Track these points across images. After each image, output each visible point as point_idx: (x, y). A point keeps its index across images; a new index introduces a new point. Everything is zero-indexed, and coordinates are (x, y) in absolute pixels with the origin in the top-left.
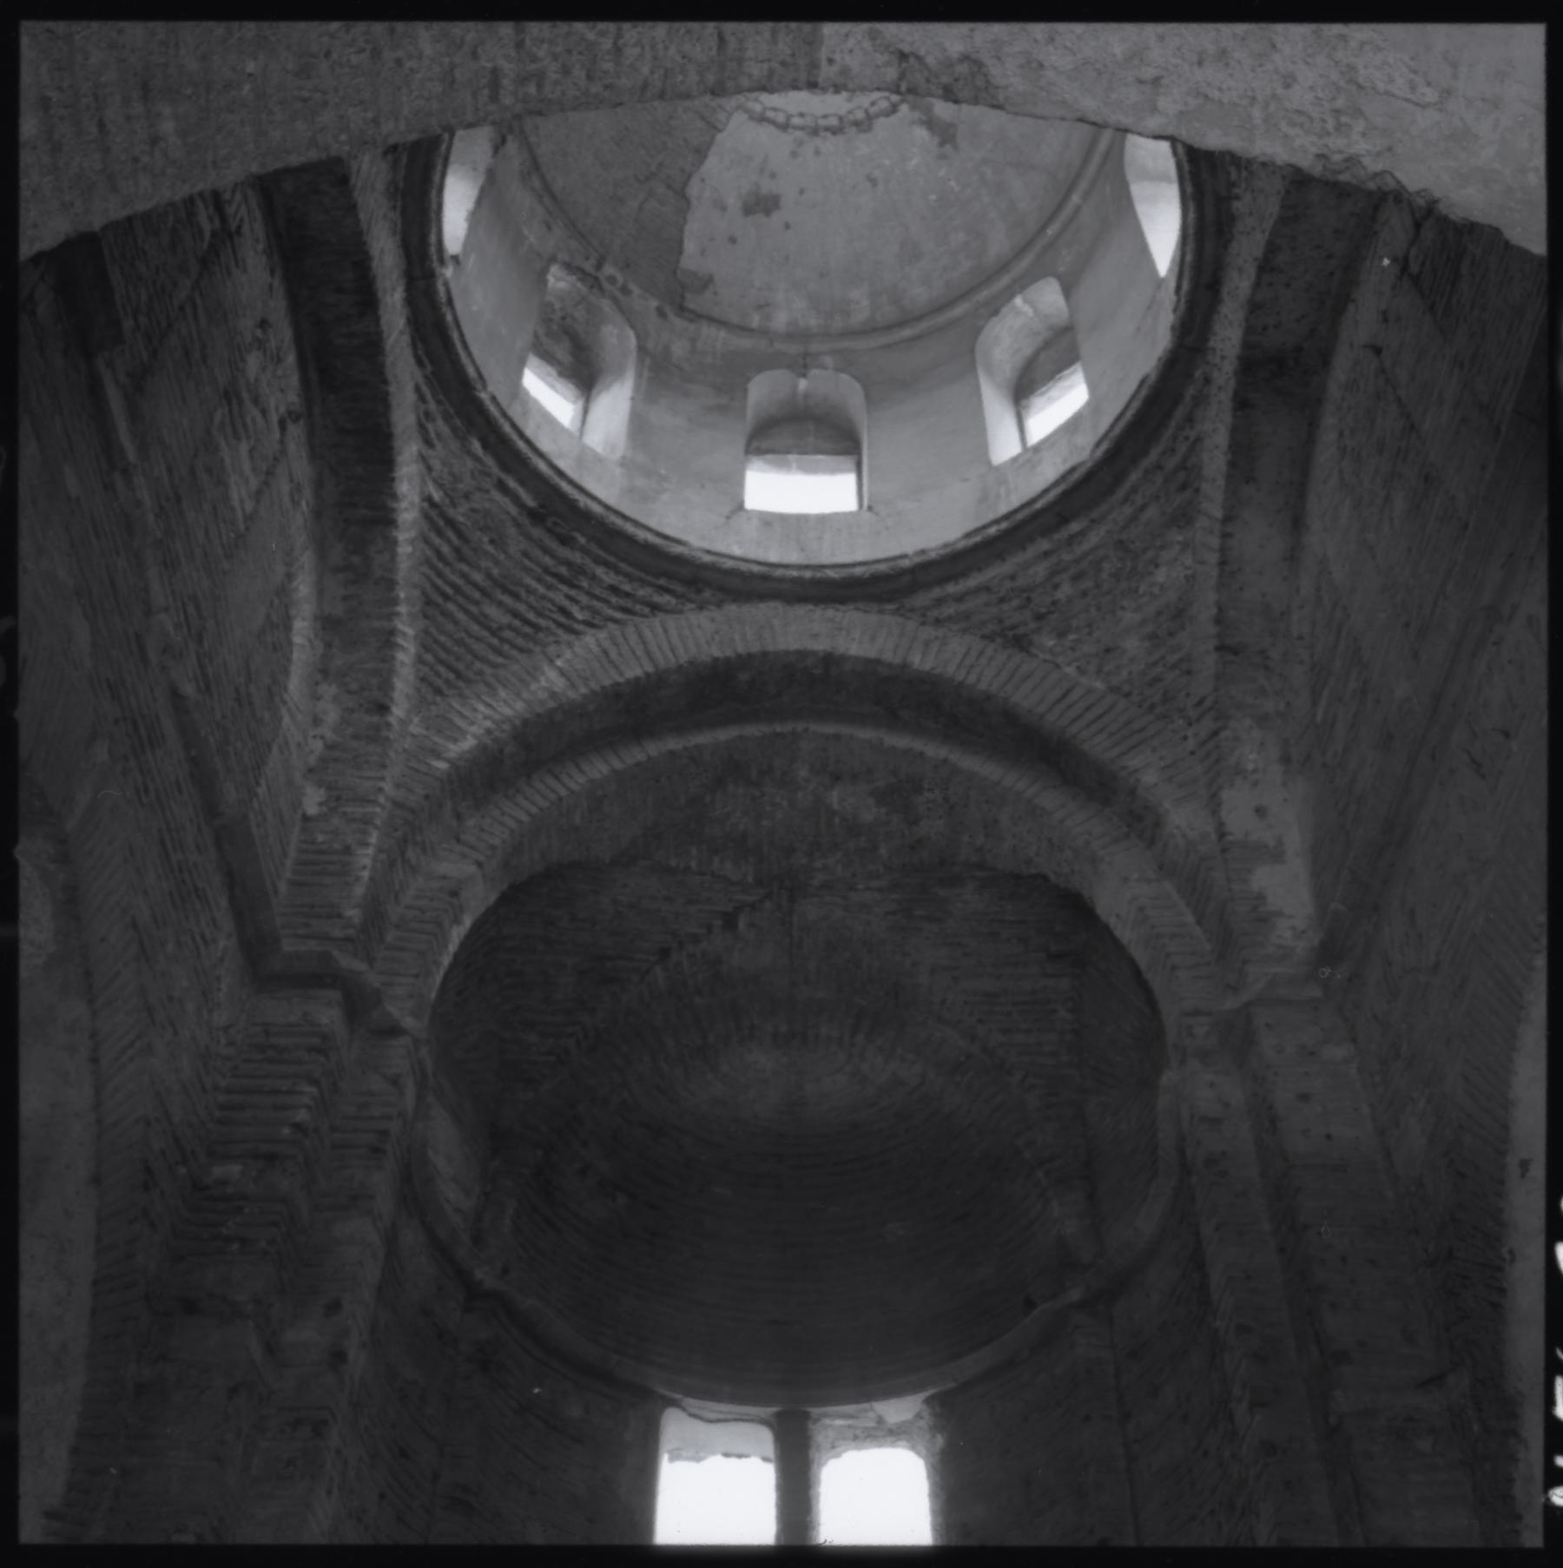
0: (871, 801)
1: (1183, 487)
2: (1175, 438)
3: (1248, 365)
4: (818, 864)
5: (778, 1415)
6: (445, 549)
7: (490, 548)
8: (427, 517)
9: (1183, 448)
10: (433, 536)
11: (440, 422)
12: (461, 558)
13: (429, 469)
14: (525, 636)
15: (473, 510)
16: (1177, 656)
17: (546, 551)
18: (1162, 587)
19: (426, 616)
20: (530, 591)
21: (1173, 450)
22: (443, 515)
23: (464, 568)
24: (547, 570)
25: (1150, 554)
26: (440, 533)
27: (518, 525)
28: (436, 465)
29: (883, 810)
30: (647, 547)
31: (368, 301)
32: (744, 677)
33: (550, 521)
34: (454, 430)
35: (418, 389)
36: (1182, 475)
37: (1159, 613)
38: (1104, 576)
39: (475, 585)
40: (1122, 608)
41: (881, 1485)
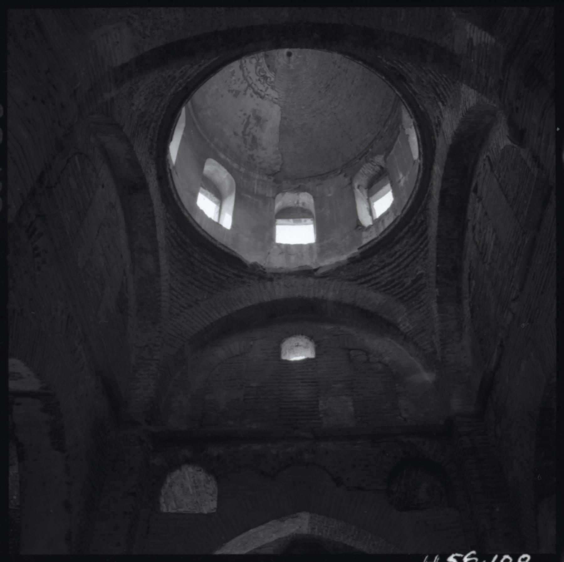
6: (442, 89)
7: (423, 80)
8: (446, 101)
11: (433, 121)
13: (440, 112)
23: (436, 81)
26: (443, 94)
31: (443, 194)
35: (438, 135)
39: (432, 74)
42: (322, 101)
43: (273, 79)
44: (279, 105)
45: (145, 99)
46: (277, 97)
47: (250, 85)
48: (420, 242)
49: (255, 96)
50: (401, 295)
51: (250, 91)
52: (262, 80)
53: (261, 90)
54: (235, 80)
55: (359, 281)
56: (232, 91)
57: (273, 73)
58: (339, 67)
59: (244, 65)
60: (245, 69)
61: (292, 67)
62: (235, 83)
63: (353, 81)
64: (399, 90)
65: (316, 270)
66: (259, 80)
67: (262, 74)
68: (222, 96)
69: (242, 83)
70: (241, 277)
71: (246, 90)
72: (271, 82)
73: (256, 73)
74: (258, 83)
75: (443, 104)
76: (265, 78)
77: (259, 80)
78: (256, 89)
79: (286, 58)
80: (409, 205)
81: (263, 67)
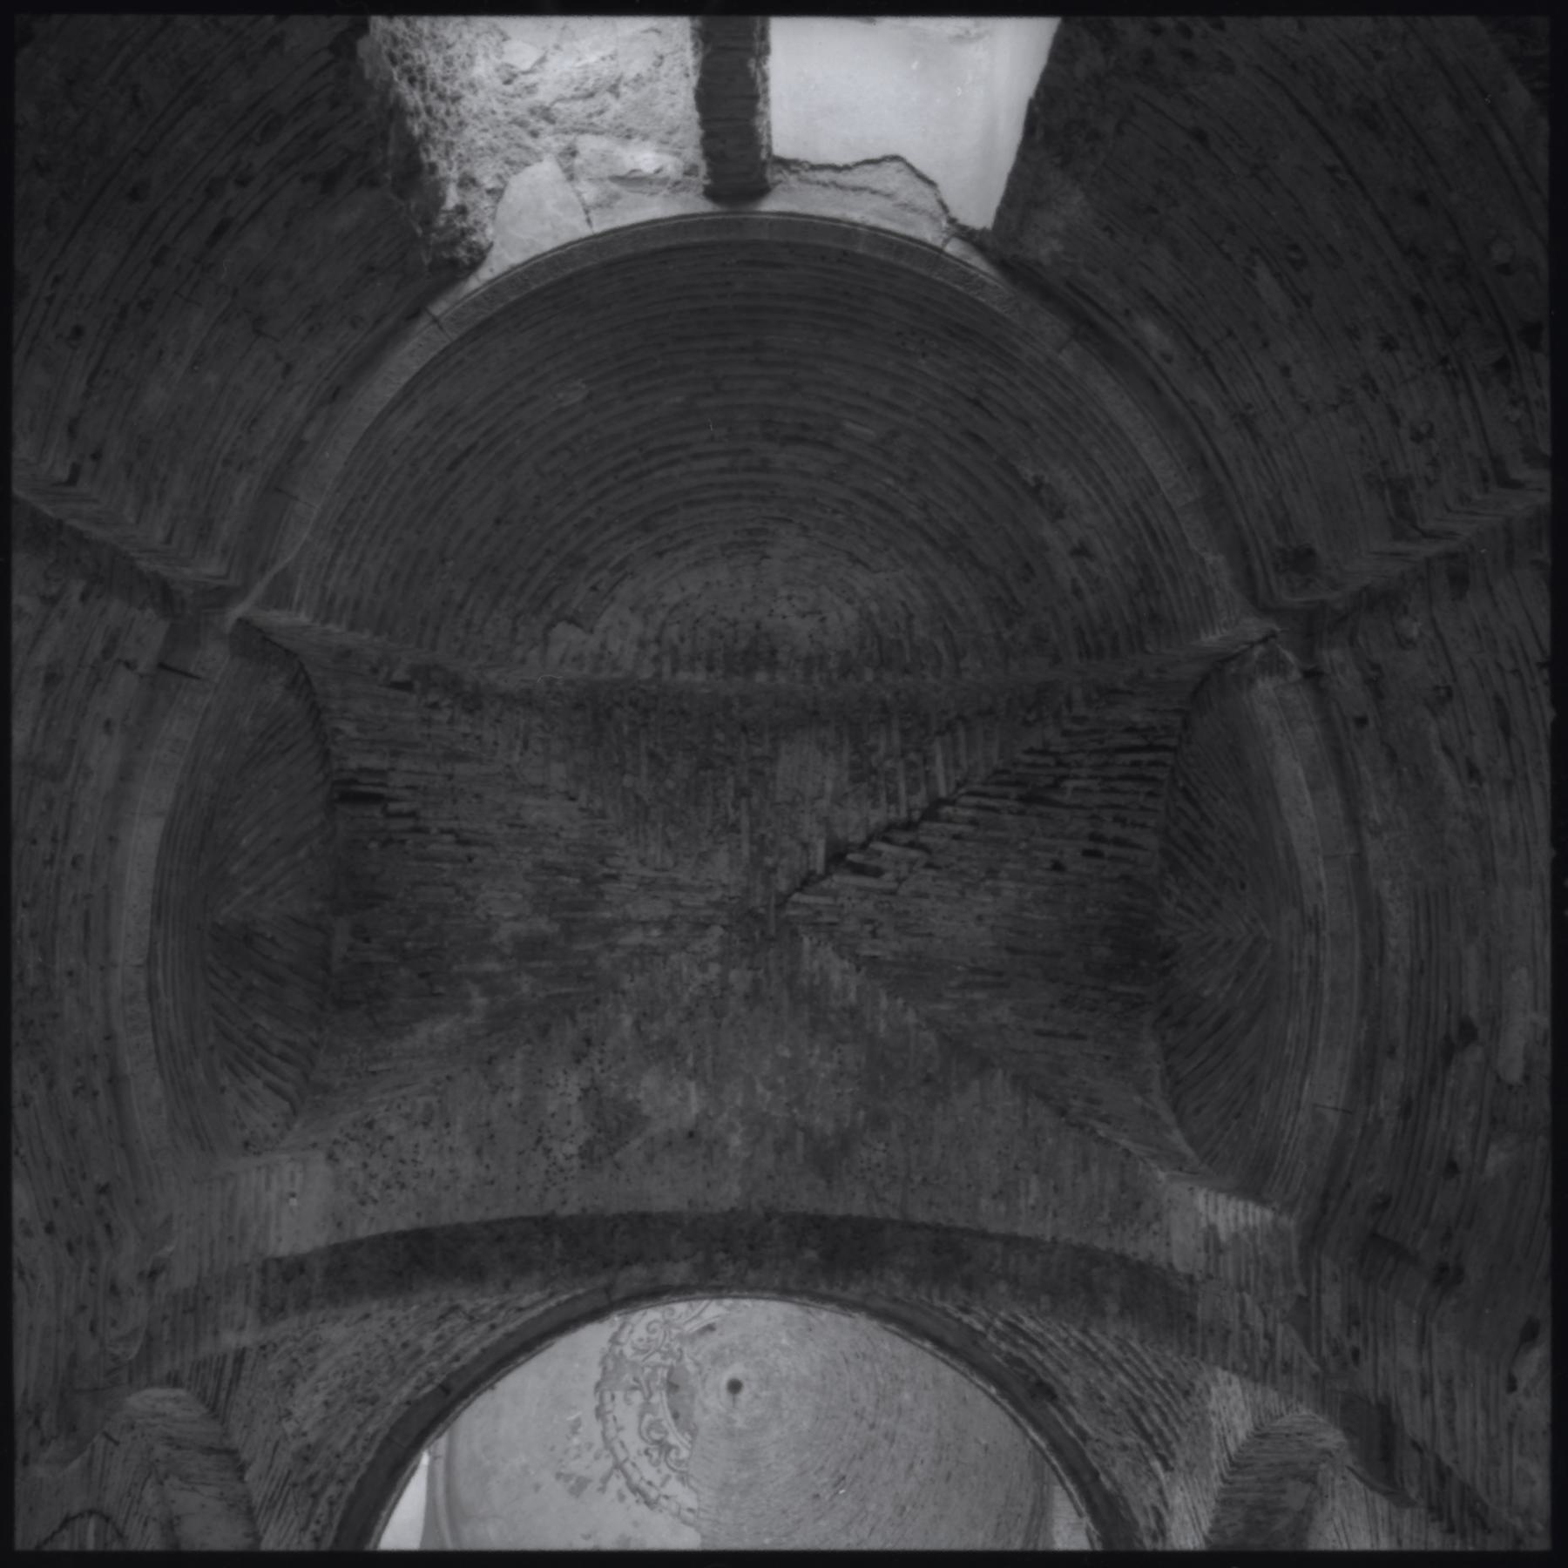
0: (647, 1109)
1: (311, 1479)
2: (331, 1514)
4: (715, 969)
5: (763, 190)
6: (1156, 1417)
7: (1104, 1393)
8: (1173, 1455)
9: (322, 1508)
10: (1169, 1436)
11: (1142, 1522)
12: (1138, 1400)
13: (1160, 1492)
15: (1118, 1433)
16: (282, 1349)
17: (1040, 1363)
18: (316, 1391)
19: (1192, 1385)
20: (1066, 1341)
21: (331, 1503)
22: (1154, 1447)
23: (1138, 1393)
24: (1042, 1349)
25: (337, 1408)
26: (1161, 1434)
27: (1072, 1400)
28: (1151, 1490)
29: (630, 1096)
30: (925, 1335)
32: (811, 1255)
33: (1033, 1379)
34: (1128, 1508)
36: (315, 1487)
37: (312, 1369)
38: (385, 1370)
39: (1127, 1374)
40: (358, 1354)
41: (558, 133)
42: (822, 1523)
43: (684, 1454)
44: (698, 1529)
45: (326, 1404)
46: (693, 1504)
47: (618, 1466)
49: (631, 1498)
51: (617, 1483)
52: (655, 1454)
53: (650, 1483)
54: (578, 1447)
56: (568, 1477)
57: (688, 1436)
58: (872, 1426)
59: (609, 1407)
60: (610, 1417)
61: (740, 1423)
62: (578, 1456)
63: (911, 1466)
64: (1038, 1428)
66: (646, 1452)
67: (656, 1436)
68: (537, 1487)
69: (597, 1458)
71: (605, 1480)
72: (679, 1462)
73: (640, 1433)
74: (643, 1462)
75: (1167, 1467)
76: (664, 1447)
77: (646, 1452)
78: (636, 1478)
79: (724, 1393)
81: (660, 1416)
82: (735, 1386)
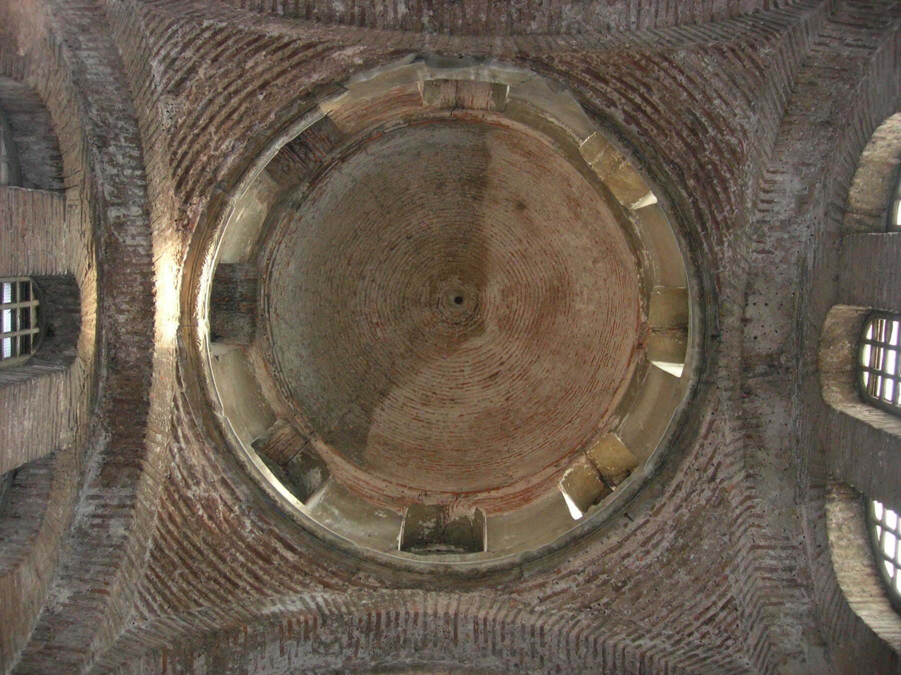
3: (746, 367)
14: (226, 589)
26: (174, 503)
48: (189, 156)
50: (219, 38)
55: (320, 48)
65: (418, 58)
70: (588, 71)
80: (220, 226)
82: (459, 300)
